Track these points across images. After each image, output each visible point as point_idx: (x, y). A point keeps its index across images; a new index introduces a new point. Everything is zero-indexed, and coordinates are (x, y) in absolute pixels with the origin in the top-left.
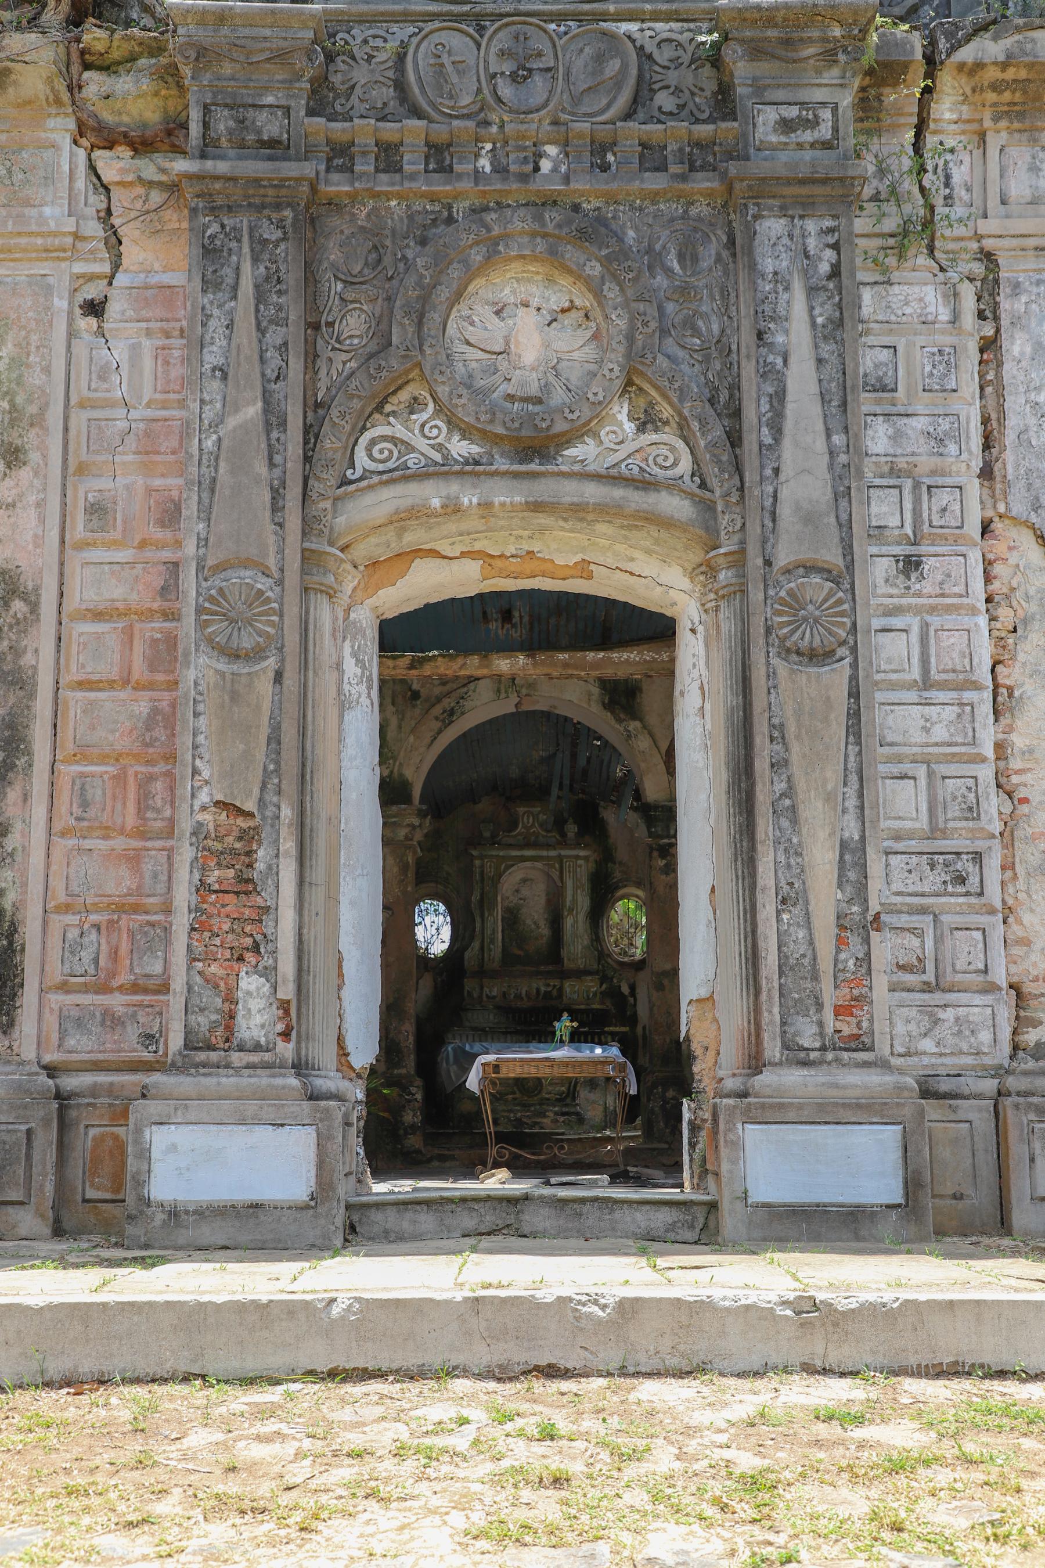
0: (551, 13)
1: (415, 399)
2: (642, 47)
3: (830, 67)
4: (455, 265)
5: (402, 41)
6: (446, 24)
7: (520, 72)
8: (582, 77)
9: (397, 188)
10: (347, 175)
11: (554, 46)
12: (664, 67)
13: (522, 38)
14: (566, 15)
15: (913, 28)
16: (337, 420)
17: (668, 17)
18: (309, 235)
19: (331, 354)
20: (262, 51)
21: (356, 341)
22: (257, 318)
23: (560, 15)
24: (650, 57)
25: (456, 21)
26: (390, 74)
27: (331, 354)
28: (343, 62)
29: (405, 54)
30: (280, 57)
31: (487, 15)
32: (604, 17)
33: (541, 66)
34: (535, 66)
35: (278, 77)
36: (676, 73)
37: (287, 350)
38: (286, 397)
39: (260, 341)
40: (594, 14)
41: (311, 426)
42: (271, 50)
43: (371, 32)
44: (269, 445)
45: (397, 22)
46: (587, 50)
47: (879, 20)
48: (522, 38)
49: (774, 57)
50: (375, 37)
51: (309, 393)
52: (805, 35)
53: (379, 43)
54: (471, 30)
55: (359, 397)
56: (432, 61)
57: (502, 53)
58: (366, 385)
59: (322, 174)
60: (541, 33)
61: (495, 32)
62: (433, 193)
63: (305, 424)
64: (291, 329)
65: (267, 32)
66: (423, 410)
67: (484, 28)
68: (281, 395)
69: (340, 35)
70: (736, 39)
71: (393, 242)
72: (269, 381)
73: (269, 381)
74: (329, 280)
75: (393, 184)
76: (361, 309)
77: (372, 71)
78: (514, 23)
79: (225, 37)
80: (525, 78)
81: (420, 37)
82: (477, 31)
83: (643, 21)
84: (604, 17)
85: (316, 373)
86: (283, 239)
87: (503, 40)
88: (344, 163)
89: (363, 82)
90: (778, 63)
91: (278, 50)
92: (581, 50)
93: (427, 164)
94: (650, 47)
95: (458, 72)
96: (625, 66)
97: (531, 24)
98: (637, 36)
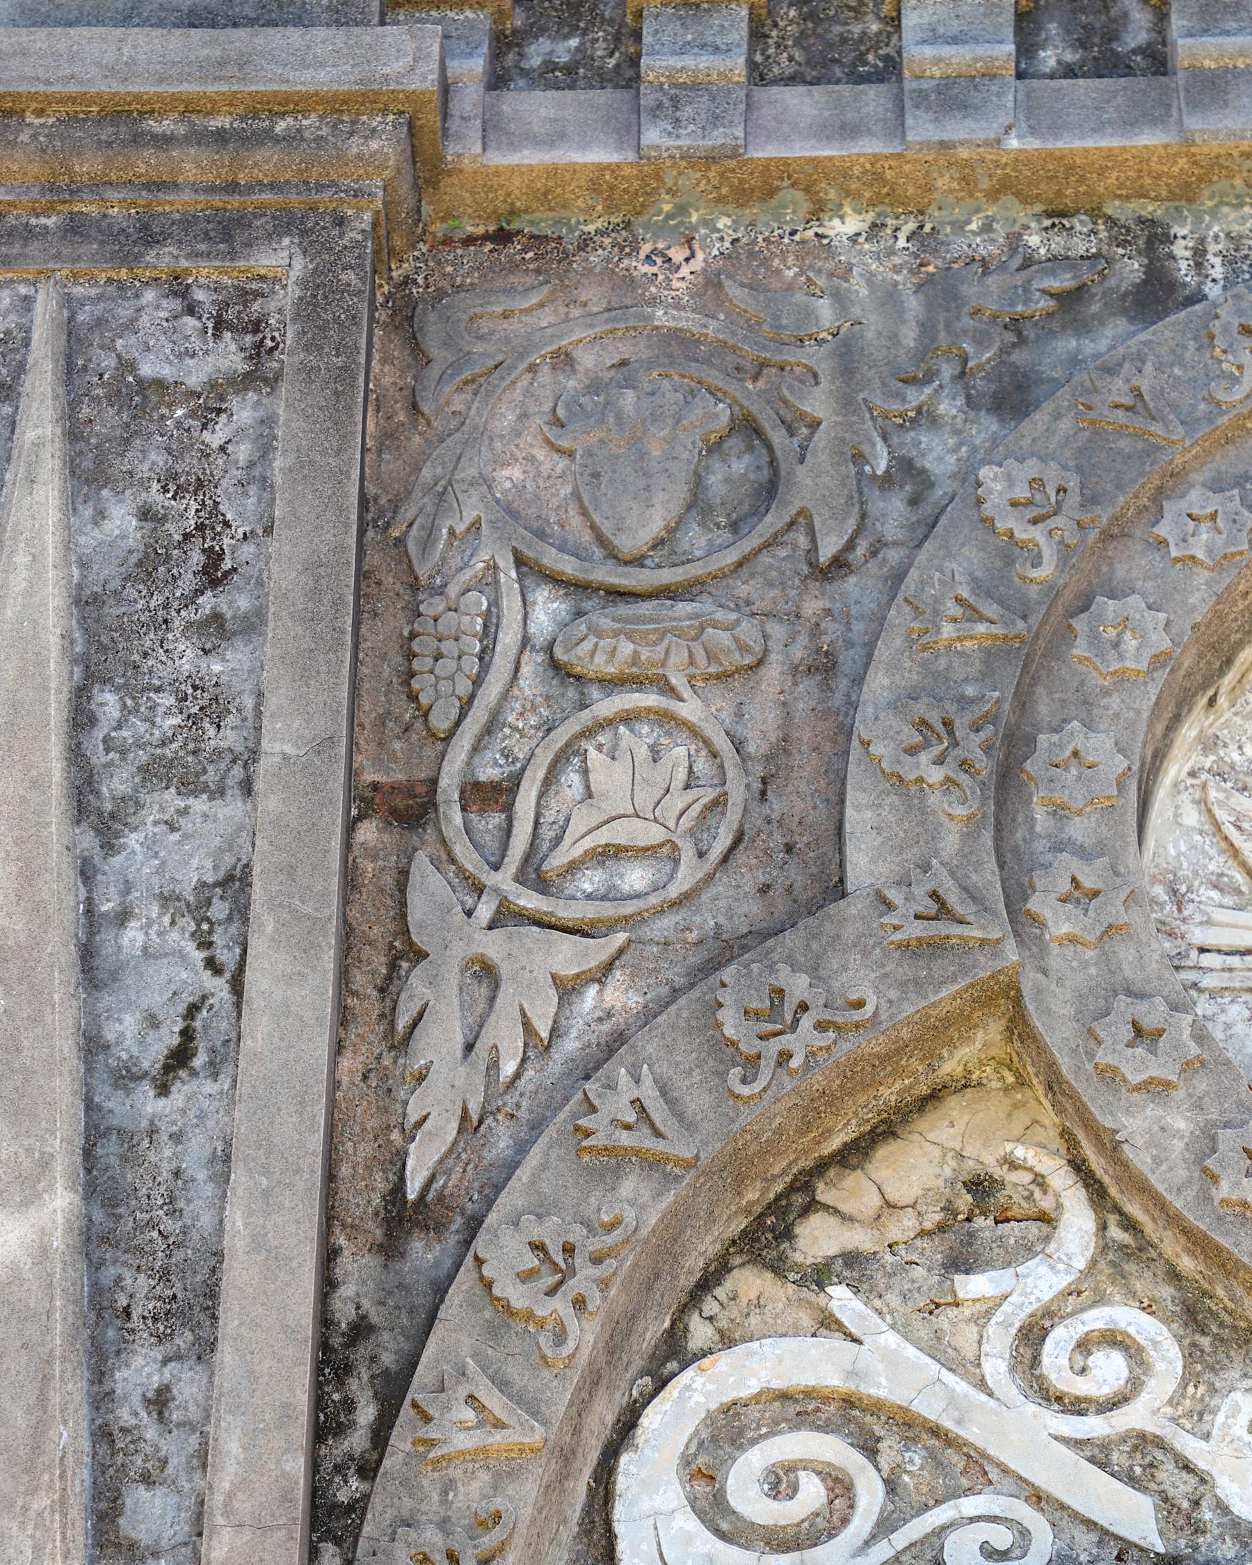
1: (981, 1187)
4: (1196, 499)
9: (870, 146)
10: (603, 97)
16: (518, 1296)
18: (387, 376)
19: (493, 946)
21: (636, 877)
22: (76, 756)
27: (493, 946)
37: (241, 912)
38: (222, 1163)
39: (87, 873)
41: (361, 1329)
44: (103, 1434)
51: (357, 1152)
55: (654, 1163)
58: (698, 1101)
59: (470, 96)
62: (1068, 167)
63: (325, 1321)
64: (270, 802)
66: (1028, 1250)
68: (198, 1148)
71: (847, 403)
72: (126, 1077)
73: (126, 1077)
74: (489, 580)
75: (849, 131)
76: (664, 718)
85: (401, 1044)
86: (246, 382)
88: (582, 57)
93: (1027, 48)
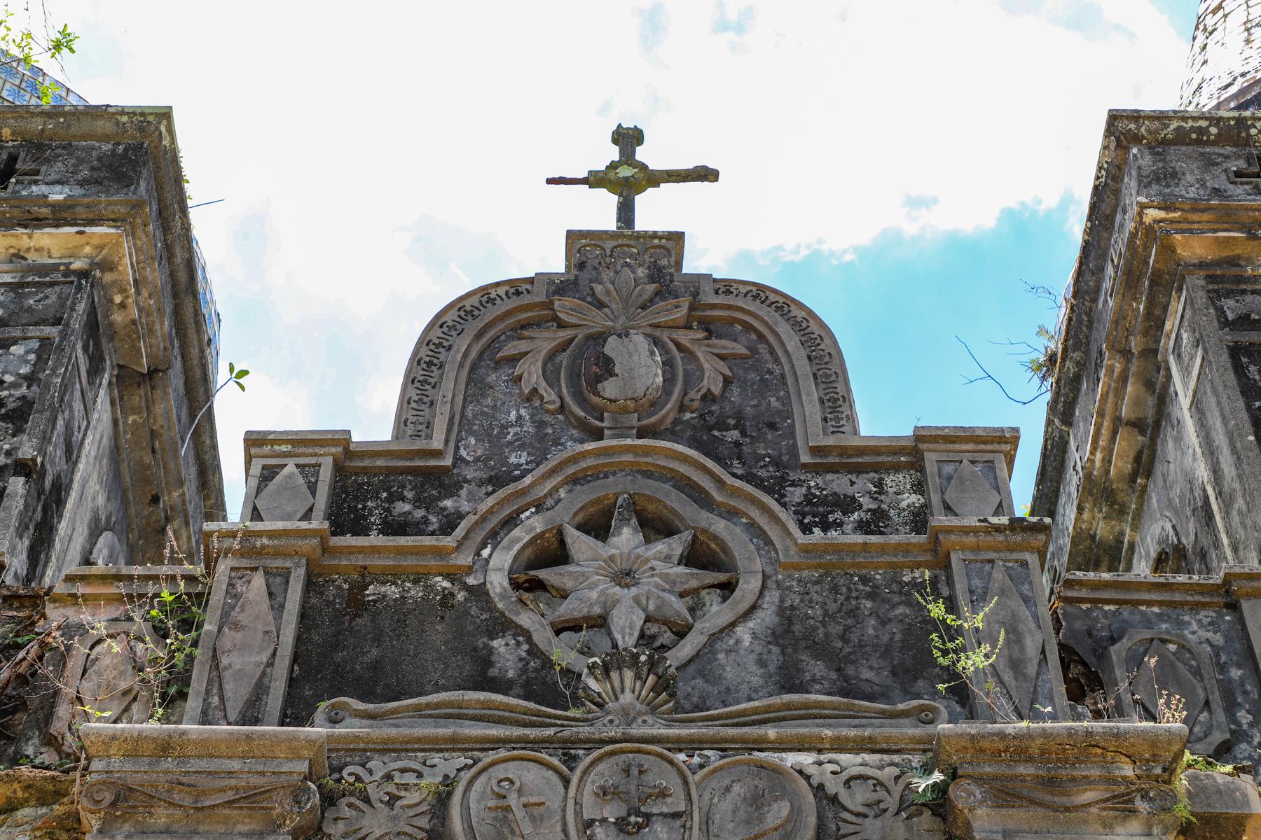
0: (679, 740)
2: (821, 787)
3: (1125, 819)
5: (446, 777)
6: (515, 752)
7: (633, 819)
8: (730, 826)
11: (686, 782)
12: (858, 815)
13: (635, 771)
14: (701, 742)
15: (1240, 770)
17: (859, 747)
20: (222, 790)
23: (692, 741)
24: (834, 799)
25: (532, 749)
26: (424, 822)
28: (350, 805)
29: (449, 794)
30: (251, 799)
31: (580, 741)
32: (761, 745)
33: (665, 810)
34: (655, 811)
35: (242, 828)
36: (878, 823)
40: (744, 741)
42: (237, 789)
43: (399, 764)
45: (441, 750)
46: (737, 788)
47: (1187, 756)
48: (635, 771)
49: (1033, 802)
50: (403, 771)
52: (1077, 773)
53: (410, 778)
54: (555, 761)
56: (491, 803)
57: (604, 793)
60: (665, 764)
61: (592, 764)
65: (236, 765)
67: (575, 758)
69: (350, 769)
70: (970, 777)
77: (395, 818)
78: (622, 752)
79: (166, 772)
80: (640, 827)
81: (474, 770)
82: (564, 762)
83: (820, 751)
84: (761, 745)
87: (606, 773)
89: (378, 833)
90: (1040, 811)
91: (249, 788)
92: (728, 789)
94: (833, 786)
95: (533, 818)
96: (796, 812)
97: (649, 753)
98: (812, 770)
